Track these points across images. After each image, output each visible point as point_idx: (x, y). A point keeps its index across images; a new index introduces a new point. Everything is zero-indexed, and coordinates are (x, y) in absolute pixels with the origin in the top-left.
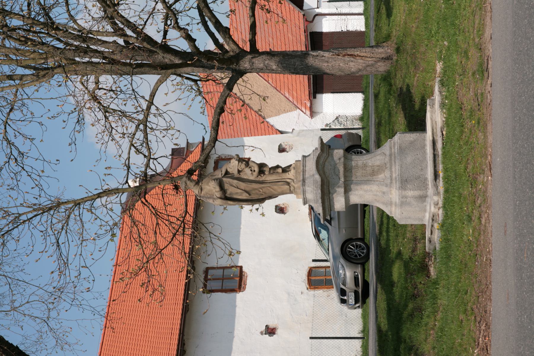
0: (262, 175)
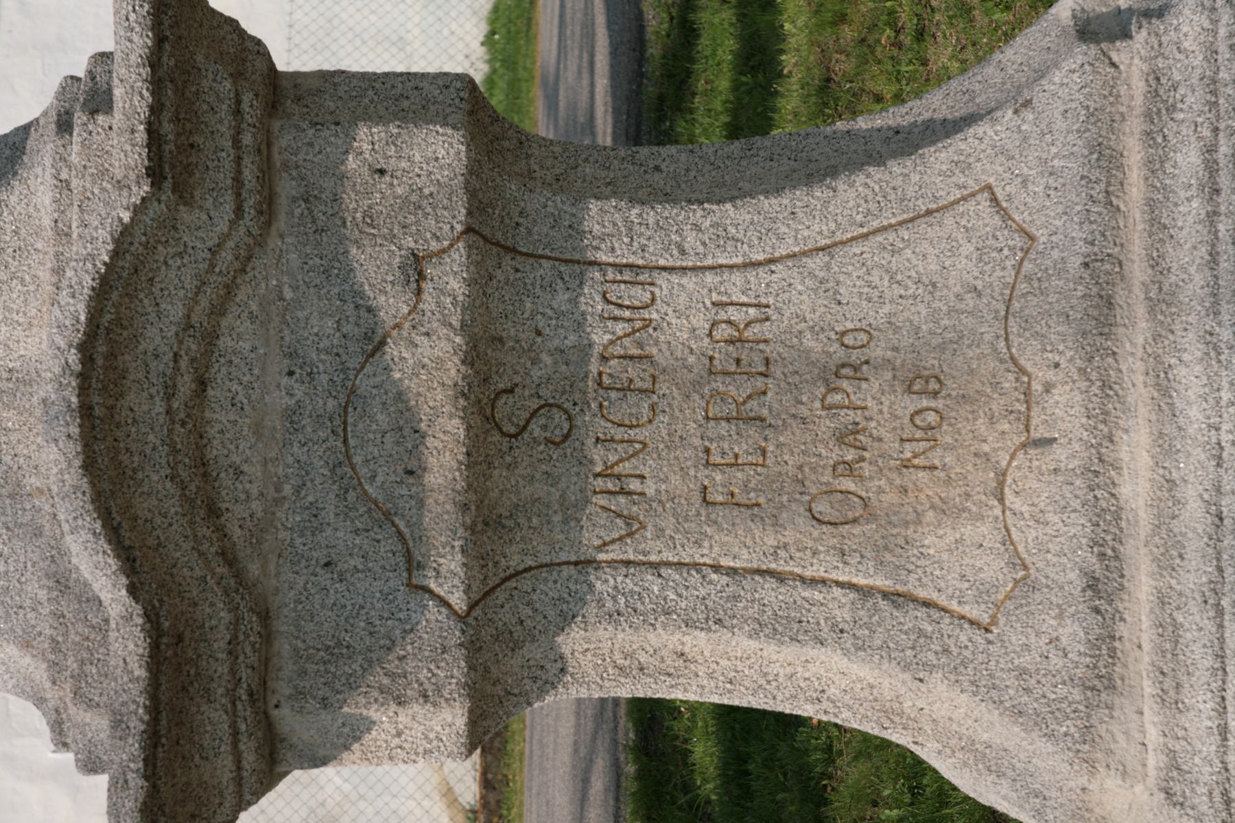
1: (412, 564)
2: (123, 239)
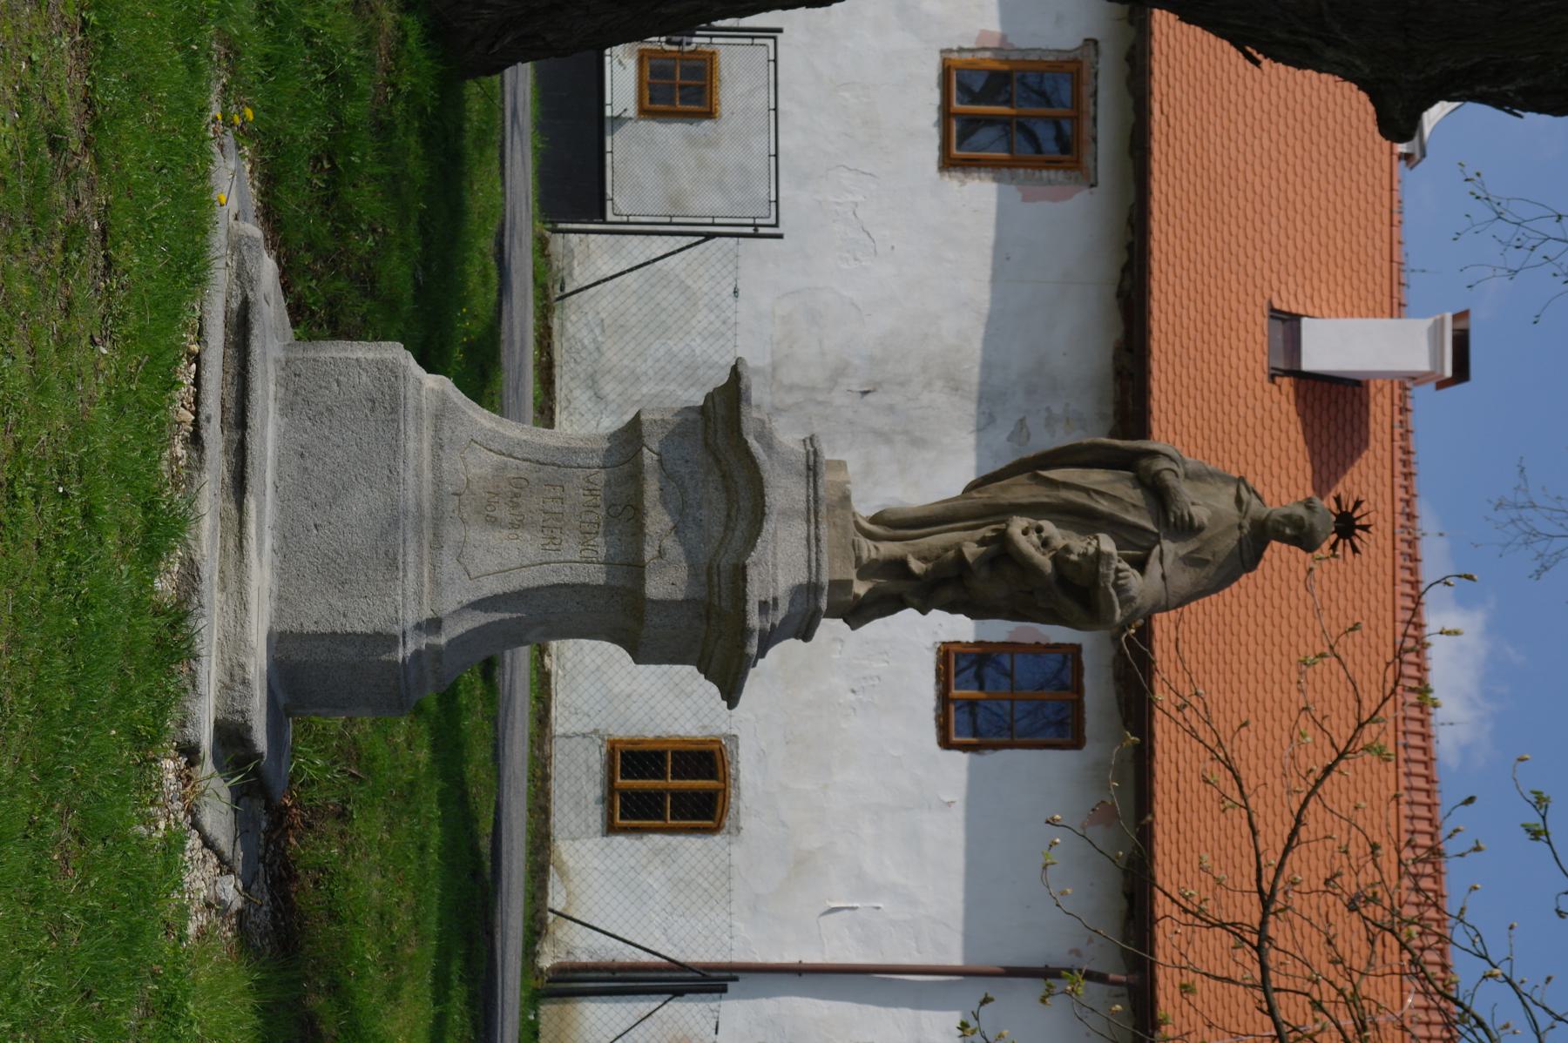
0: (989, 534)
1: (660, 461)
2: (753, 546)
